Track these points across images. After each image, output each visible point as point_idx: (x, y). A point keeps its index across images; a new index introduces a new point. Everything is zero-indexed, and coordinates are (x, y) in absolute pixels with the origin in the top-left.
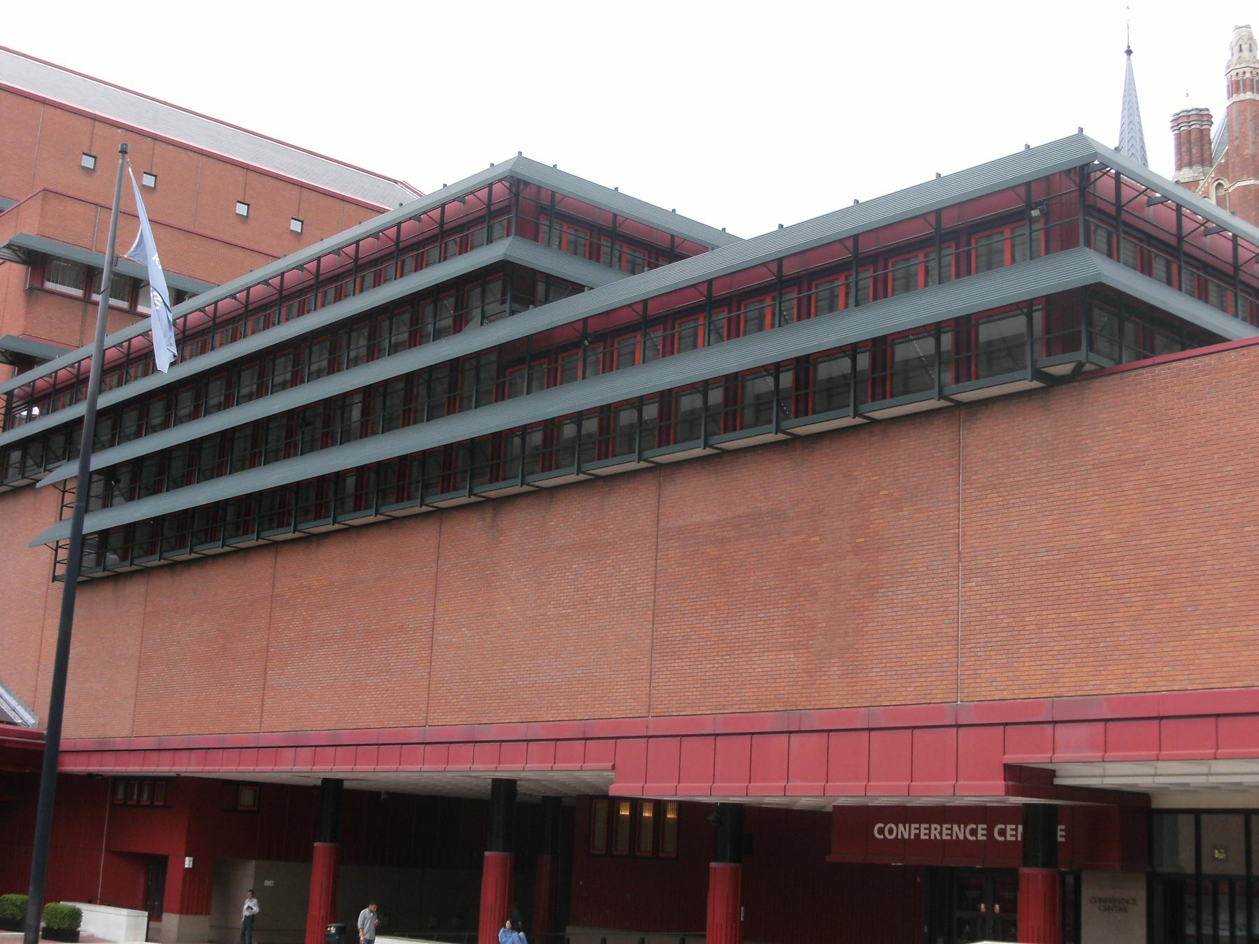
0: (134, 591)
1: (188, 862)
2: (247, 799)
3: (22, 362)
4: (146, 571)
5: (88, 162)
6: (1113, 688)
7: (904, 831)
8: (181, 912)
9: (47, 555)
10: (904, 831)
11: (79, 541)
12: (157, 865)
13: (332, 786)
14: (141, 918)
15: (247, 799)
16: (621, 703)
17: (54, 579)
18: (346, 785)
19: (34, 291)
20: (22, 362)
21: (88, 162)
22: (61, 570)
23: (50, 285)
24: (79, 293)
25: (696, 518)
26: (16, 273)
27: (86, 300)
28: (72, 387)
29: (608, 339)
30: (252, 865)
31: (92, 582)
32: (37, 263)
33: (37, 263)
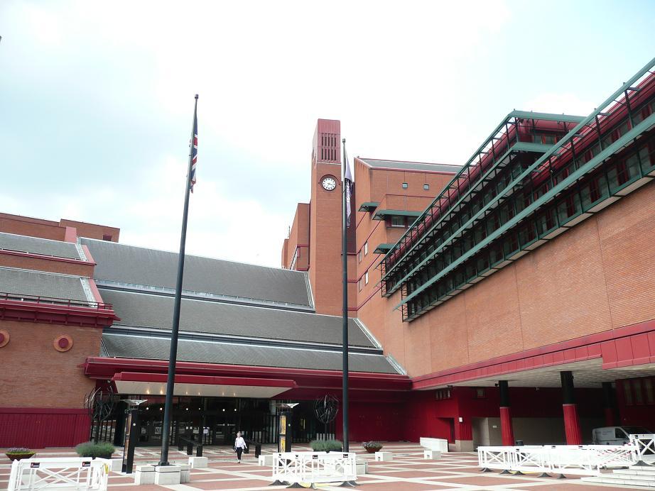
0: (426, 319)
1: (461, 420)
2: (480, 393)
4: (429, 312)
5: (405, 186)
8: (461, 440)
12: (451, 422)
14: (445, 442)
15: (480, 393)
16: (599, 326)
17: (403, 321)
18: (510, 384)
20: (385, 251)
21: (405, 186)
24: (404, 226)
25: (616, 232)
29: (561, 168)
30: (487, 419)
32: (388, 219)
33: (388, 219)
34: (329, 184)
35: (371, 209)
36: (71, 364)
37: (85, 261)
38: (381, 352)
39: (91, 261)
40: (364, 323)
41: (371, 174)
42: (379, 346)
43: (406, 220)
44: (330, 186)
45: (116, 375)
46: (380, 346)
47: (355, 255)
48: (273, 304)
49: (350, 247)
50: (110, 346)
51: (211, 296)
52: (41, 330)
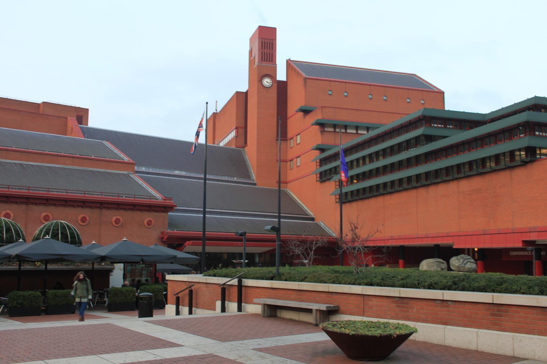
3: (322, 150)
5: (330, 93)
6: (539, 225)
7: (516, 253)
9: (334, 197)
10: (516, 253)
11: (340, 195)
13: (402, 247)
19: (323, 132)
21: (330, 93)
22: (338, 200)
23: (326, 129)
26: (317, 127)
27: (335, 131)
28: (335, 157)
31: (344, 203)
32: (322, 125)
33: (322, 125)
34: (267, 82)
35: (306, 112)
36: (155, 234)
37: (126, 161)
38: (313, 219)
39: (131, 161)
40: (292, 192)
41: (305, 83)
42: (312, 214)
43: (335, 126)
44: (267, 84)
45: (187, 242)
46: (312, 214)
47: (287, 140)
48: (226, 178)
49: (282, 133)
50: (172, 225)
51: (184, 173)
52: (137, 215)
